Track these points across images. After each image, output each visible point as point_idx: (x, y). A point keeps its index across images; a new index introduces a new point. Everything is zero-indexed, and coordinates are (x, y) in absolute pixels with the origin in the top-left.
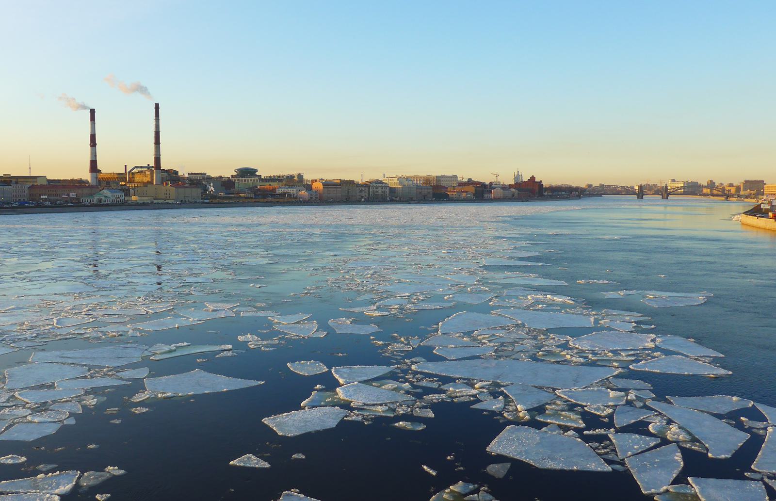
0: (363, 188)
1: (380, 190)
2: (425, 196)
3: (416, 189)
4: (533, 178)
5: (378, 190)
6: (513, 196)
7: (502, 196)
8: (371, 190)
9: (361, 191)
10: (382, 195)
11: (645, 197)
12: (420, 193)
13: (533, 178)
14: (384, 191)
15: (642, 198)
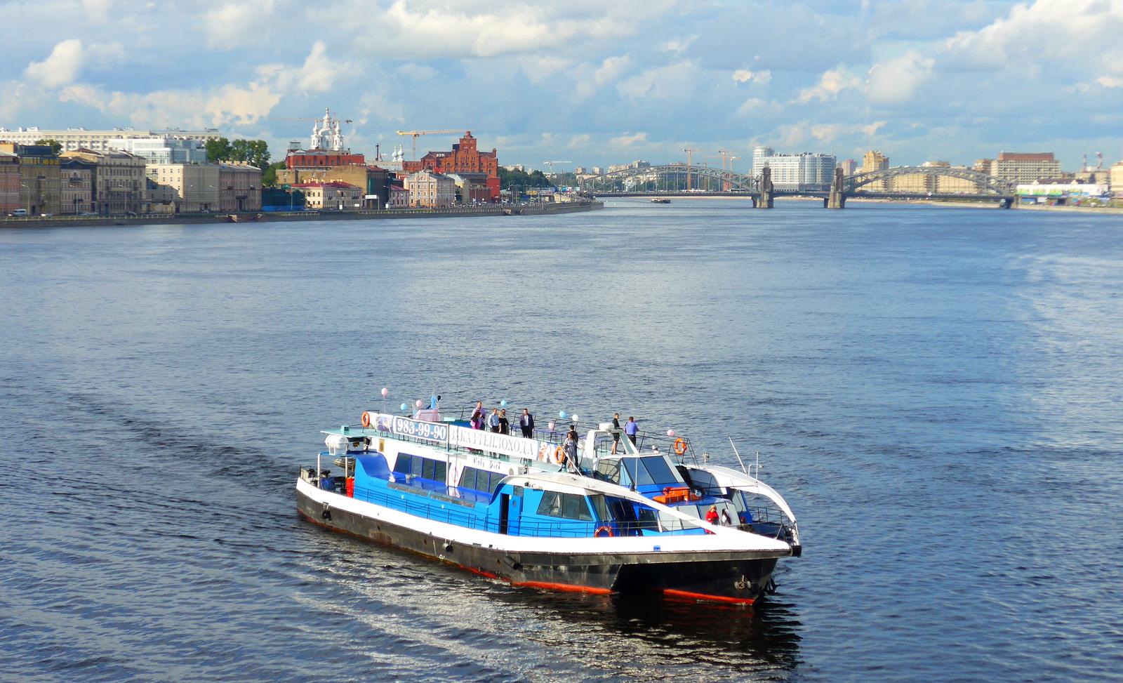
0: (78, 172)
1: (124, 178)
2: (241, 200)
3: (217, 175)
4: (469, 141)
5: (118, 178)
6: (459, 197)
7: (435, 196)
8: (99, 179)
9: (75, 181)
10: (129, 194)
11: (778, 201)
12: (230, 188)
13: (469, 141)
14: (135, 182)
15: (770, 205)
